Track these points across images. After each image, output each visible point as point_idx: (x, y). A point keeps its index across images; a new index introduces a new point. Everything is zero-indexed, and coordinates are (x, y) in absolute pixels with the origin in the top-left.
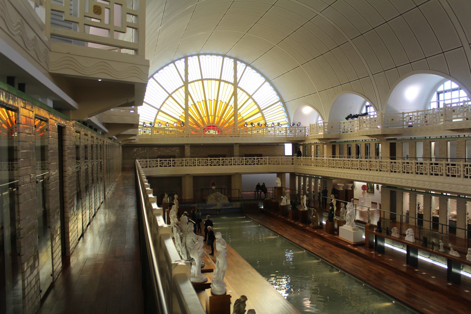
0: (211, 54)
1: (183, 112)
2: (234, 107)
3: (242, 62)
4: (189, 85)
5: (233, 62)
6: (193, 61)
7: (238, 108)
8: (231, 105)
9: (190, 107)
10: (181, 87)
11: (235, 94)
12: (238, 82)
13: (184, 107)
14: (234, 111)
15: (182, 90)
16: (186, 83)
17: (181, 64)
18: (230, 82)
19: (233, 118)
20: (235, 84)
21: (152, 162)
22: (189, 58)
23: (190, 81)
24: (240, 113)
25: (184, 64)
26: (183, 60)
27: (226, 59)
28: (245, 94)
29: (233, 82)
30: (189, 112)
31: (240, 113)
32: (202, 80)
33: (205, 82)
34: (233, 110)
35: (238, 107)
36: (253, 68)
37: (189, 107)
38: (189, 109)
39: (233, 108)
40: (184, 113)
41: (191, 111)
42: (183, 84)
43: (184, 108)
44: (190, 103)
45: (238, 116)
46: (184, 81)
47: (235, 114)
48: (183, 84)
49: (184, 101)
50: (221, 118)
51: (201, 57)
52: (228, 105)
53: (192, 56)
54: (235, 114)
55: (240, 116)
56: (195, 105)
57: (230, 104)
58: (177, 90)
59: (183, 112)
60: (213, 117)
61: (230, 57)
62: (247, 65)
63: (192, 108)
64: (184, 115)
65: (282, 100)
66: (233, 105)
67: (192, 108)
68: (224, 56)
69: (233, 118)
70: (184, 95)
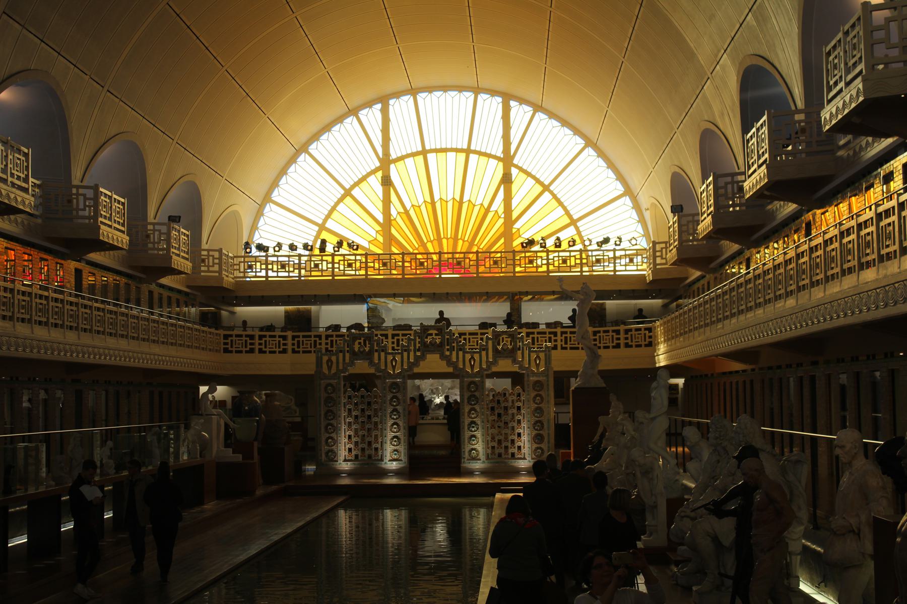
0: (445, 88)
1: (377, 232)
2: (503, 216)
3: (522, 101)
4: (392, 166)
5: (501, 104)
6: (401, 108)
7: (514, 216)
8: (496, 211)
9: (395, 219)
10: (373, 172)
11: (507, 180)
12: (512, 153)
13: (380, 218)
14: (505, 223)
15: (375, 181)
16: (386, 162)
17: (372, 116)
18: (493, 153)
19: (502, 241)
20: (507, 159)
21: (268, 339)
22: (391, 102)
23: (393, 156)
24: (519, 230)
25: (379, 116)
26: (379, 106)
27: (482, 97)
28: (531, 181)
29: (500, 154)
30: (393, 231)
31: (519, 230)
32: (424, 152)
33: (431, 157)
34: (501, 221)
35: (514, 216)
36: (552, 115)
37: (392, 218)
38: (393, 223)
39: (500, 217)
40: (381, 233)
41: (398, 228)
42: (378, 164)
43: (382, 221)
44: (395, 209)
45: (515, 237)
46: (381, 157)
47: (508, 232)
48: (378, 164)
49: (380, 205)
50: (472, 243)
51: (421, 97)
52: (487, 211)
53: (397, 95)
54: (508, 232)
55: (520, 236)
56: (407, 212)
57: (493, 208)
58: (364, 179)
59: (377, 232)
60: (451, 241)
61: (493, 93)
62: (538, 108)
63: (399, 220)
64: (381, 239)
65: (628, 192)
66: (501, 211)
67: (399, 220)
68: (477, 90)
69: (502, 241)
70: (379, 189)
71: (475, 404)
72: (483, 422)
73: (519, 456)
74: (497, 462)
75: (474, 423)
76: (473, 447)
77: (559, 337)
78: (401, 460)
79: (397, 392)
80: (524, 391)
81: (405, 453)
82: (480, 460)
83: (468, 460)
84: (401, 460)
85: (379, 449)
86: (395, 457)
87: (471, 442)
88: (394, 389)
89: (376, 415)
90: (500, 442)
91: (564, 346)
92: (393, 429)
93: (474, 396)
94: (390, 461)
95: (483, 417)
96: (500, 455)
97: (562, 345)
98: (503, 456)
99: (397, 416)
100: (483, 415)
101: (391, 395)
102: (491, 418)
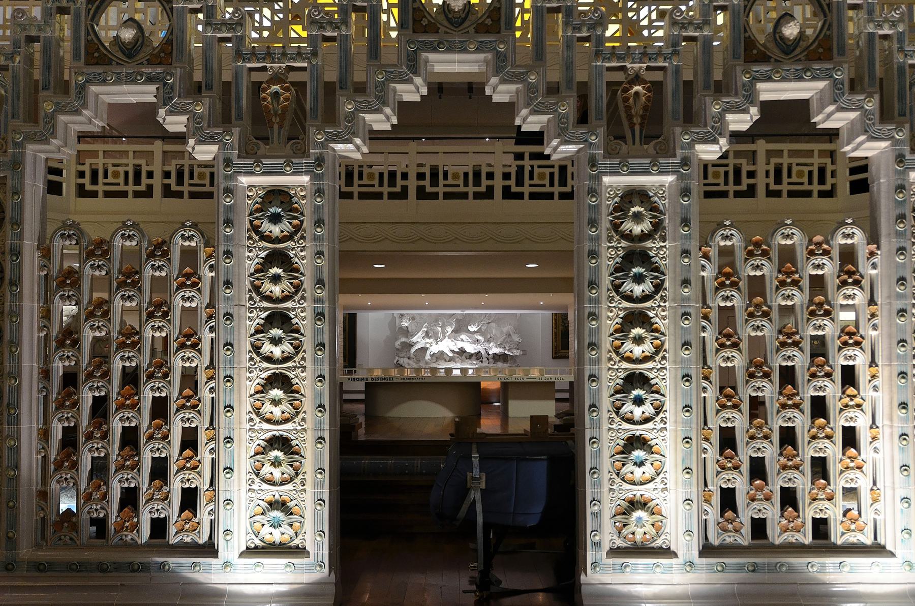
71: (645, 298)
72: (687, 377)
73: (852, 538)
74: (755, 568)
75: (642, 380)
76: (638, 492)
77: (761, 167)
78: (300, 551)
79: (290, 237)
80: (874, 238)
81: (317, 515)
82: (666, 552)
83: (615, 552)
84: (300, 551)
85: (202, 499)
86: (277, 536)
87: (630, 467)
88: (275, 219)
89: (190, 341)
90: (758, 469)
91: (773, 187)
92: (268, 408)
93: (644, 258)
94: (251, 552)
95: (685, 354)
96: (759, 527)
97: (767, 185)
98: (775, 536)
99: (287, 347)
100: (686, 344)
101: (262, 250)
102: (717, 361)
